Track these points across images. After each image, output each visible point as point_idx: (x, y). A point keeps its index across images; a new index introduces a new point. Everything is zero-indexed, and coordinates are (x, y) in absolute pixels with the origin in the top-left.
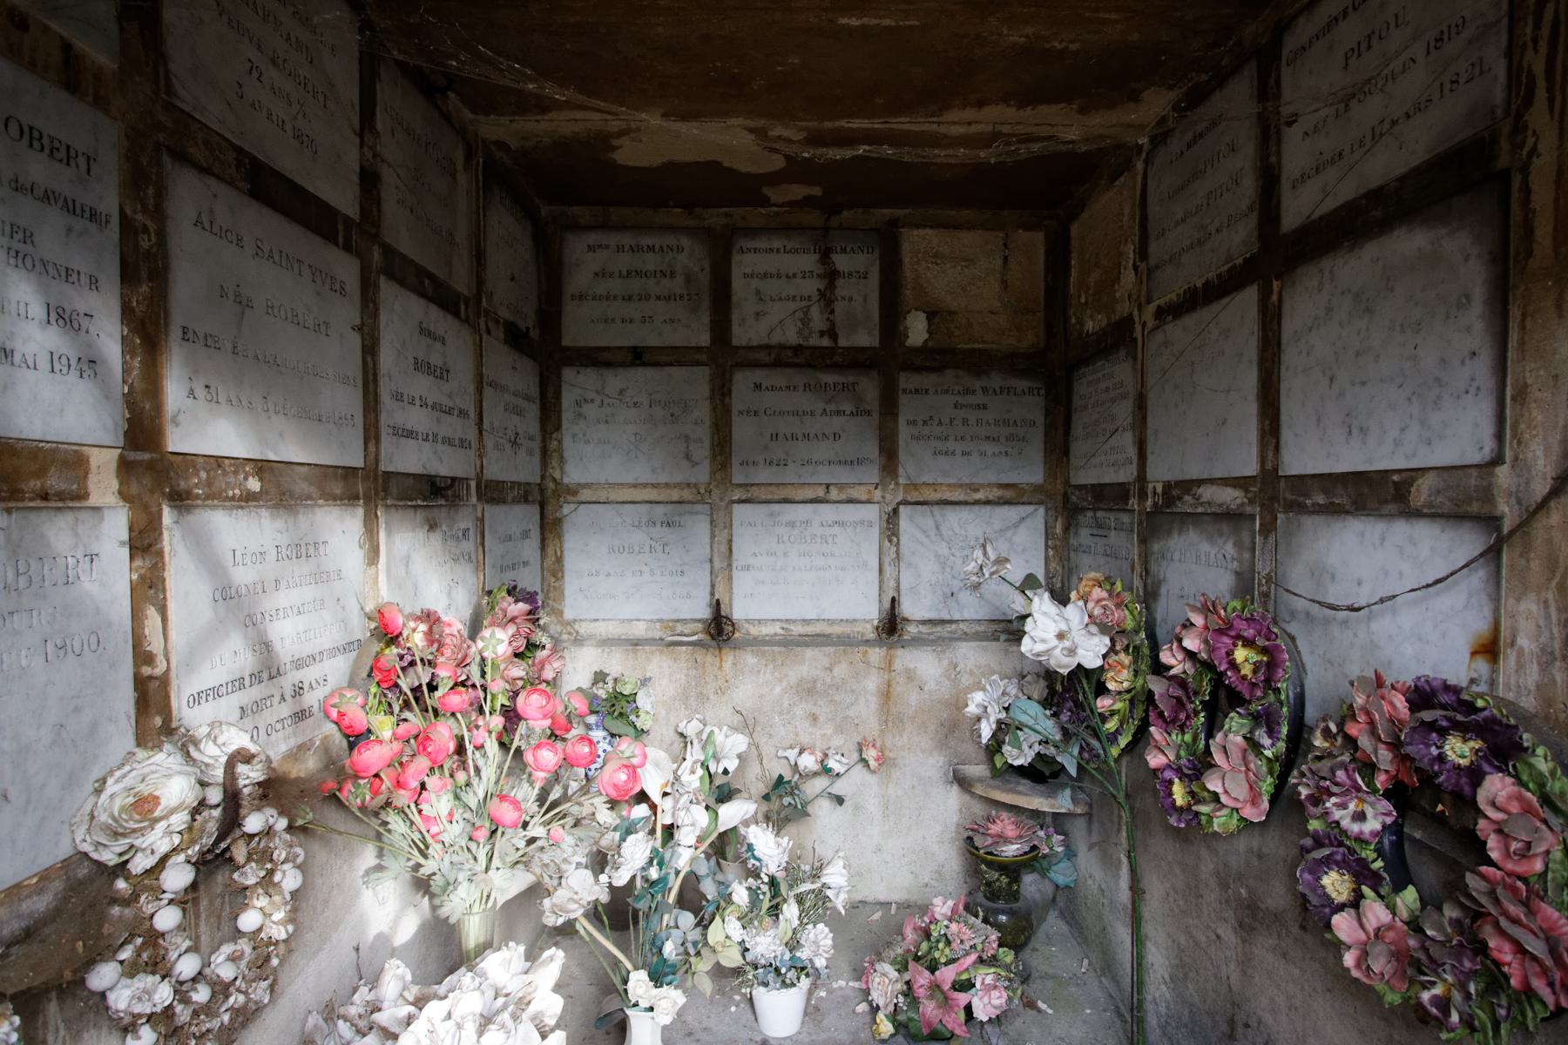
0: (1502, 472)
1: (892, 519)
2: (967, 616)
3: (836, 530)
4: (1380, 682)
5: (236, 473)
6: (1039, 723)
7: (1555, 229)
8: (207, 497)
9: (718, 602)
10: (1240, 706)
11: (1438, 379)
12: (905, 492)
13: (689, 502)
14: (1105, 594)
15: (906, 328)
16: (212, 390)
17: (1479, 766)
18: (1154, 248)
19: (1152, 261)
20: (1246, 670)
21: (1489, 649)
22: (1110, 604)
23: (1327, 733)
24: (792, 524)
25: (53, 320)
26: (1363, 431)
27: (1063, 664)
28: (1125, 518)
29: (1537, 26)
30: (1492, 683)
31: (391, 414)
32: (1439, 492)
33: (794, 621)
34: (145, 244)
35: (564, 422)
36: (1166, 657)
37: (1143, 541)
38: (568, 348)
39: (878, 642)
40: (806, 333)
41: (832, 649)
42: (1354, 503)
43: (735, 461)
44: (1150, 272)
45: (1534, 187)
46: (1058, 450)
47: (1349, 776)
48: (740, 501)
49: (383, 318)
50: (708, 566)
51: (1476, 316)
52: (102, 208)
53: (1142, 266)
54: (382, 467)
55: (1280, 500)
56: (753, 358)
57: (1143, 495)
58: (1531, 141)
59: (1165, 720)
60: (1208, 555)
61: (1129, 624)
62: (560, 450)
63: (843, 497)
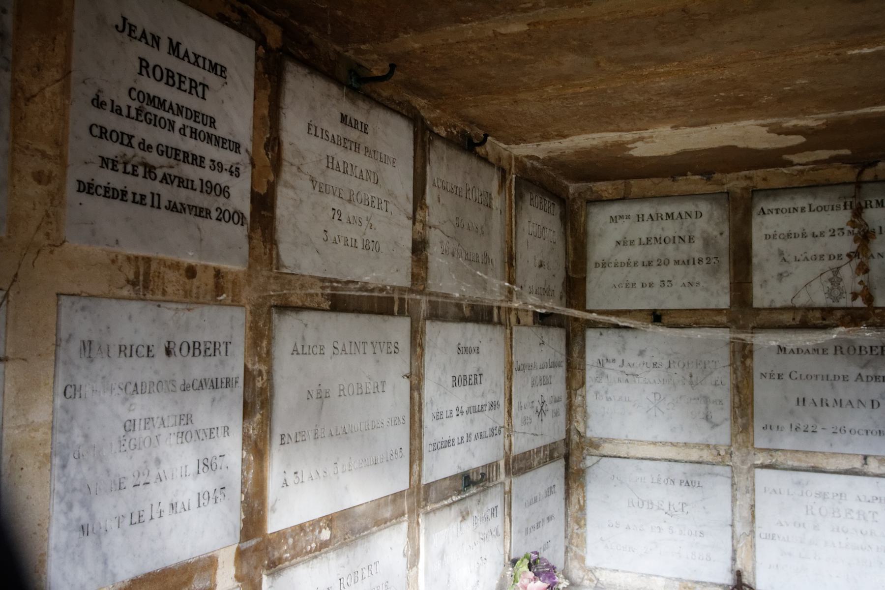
5: (313, 531)
8: (293, 557)
13: (707, 463)
16: (299, 475)
24: (823, 496)
25: (201, 471)
31: (433, 431)
34: (259, 384)
35: (588, 379)
40: (836, 292)
48: (764, 466)
49: (427, 357)
50: (729, 529)
52: (233, 375)
54: (424, 482)
62: (584, 405)
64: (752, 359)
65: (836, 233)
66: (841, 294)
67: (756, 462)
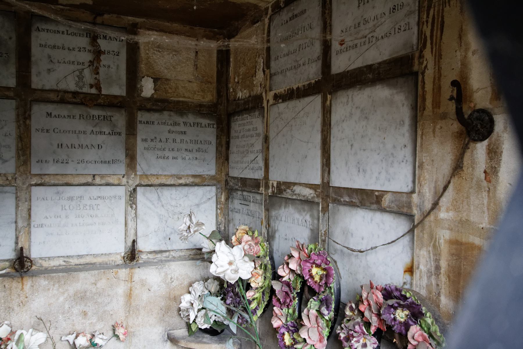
0: (415, 196)
1: (133, 194)
2: (175, 247)
3: (99, 201)
4: (372, 287)
6: (217, 307)
7: (433, 101)
9: (22, 249)
10: (314, 296)
11: (392, 154)
12: (140, 179)
14: (250, 238)
15: (142, 86)
17: (408, 322)
18: (273, 64)
19: (273, 71)
20: (317, 279)
21: (410, 270)
22: (252, 243)
23: (351, 309)
24: (71, 199)
26: (364, 171)
27: (231, 278)
28: (258, 197)
29: (428, 17)
30: (411, 284)
32: (392, 202)
33: (72, 257)
36: (280, 272)
37: (267, 210)
39: (125, 265)
41: (96, 272)
42: (361, 202)
43: (33, 160)
44: (271, 76)
45: (426, 82)
46: (224, 155)
47: (360, 328)
48: (36, 185)
50: (14, 225)
51: (406, 129)
53: (267, 71)
55: (329, 197)
56: (45, 97)
57: (267, 187)
58: (425, 62)
59: (280, 303)
60: (298, 220)
61: (261, 253)
63: (103, 182)
65: (82, 50)
66: (84, 85)
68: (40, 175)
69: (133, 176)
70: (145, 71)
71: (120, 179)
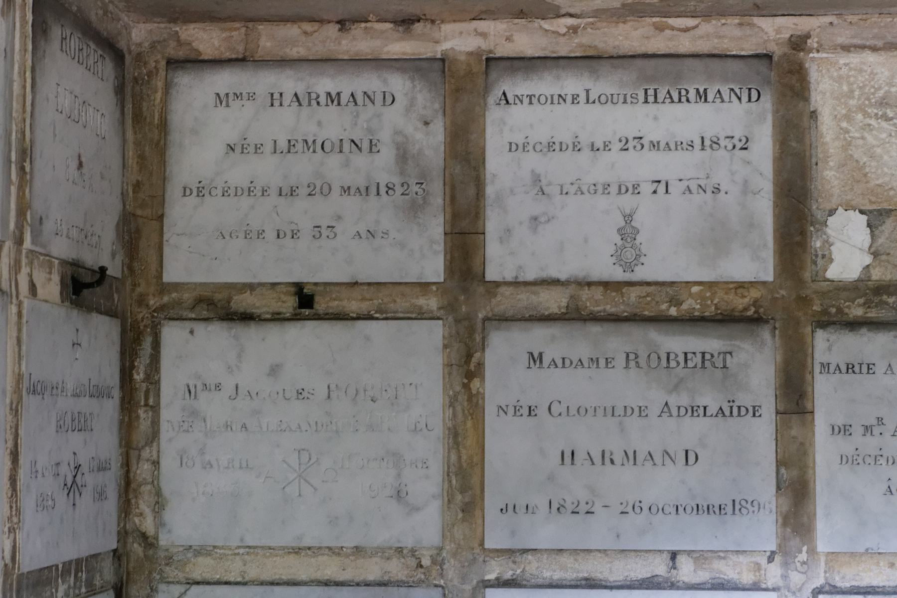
13: (399, 584)
15: (828, 243)
35: (164, 426)
38: (176, 286)
43: (492, 503)
63: (703, 576)
64: (483, 380)
65: (630, 145)
66: (638, 256)
67: (487, 577)
68: (510, 552)
69: (803, 556)
70: (836, 191)
71: (758, 567)
